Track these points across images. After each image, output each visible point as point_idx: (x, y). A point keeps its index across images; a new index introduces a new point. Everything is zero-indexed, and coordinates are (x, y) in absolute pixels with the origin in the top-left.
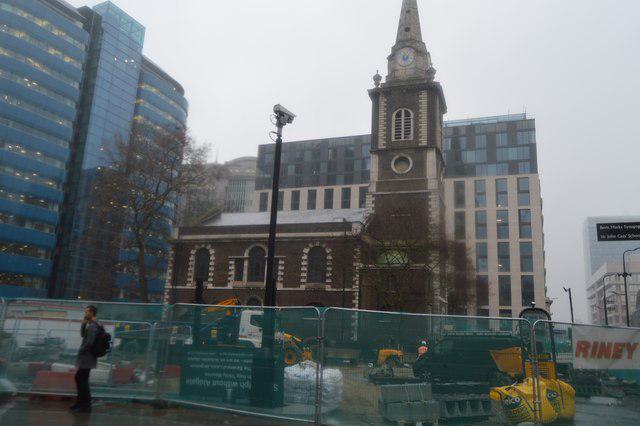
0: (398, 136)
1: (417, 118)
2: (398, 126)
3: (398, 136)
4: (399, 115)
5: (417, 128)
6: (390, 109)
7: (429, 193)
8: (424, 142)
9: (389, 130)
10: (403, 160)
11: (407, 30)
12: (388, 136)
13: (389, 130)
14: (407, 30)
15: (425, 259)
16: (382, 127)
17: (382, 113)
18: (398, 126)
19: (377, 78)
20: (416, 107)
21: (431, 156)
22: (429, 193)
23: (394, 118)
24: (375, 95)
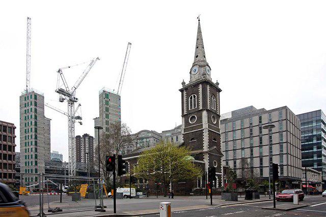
0: (191, 107)
1: (198, 97)
2: (191, 102)
3: (191, 107)
4: (191, 98)
5: (198, 102)
6: (188, 96)
7: (203, 130)
8: (201, 108)
9: (188, 106)
10: (193, 117)
11: (197, 56)
12: (188, 108)
13: (188, 106)
14: (197, 56)
15: (202, 159)
16: (185, 105)
17: (185, 99)
18: (191, 102)
19: (183, 83)
20: (197, 93)
21: (205, 114)
22: (203, 130)
23: (189, 100)
24: (181, 91)
